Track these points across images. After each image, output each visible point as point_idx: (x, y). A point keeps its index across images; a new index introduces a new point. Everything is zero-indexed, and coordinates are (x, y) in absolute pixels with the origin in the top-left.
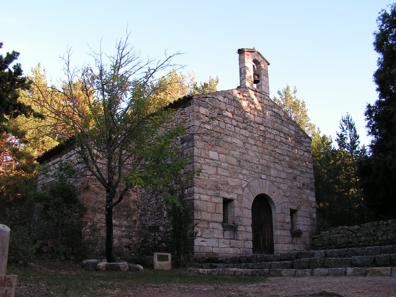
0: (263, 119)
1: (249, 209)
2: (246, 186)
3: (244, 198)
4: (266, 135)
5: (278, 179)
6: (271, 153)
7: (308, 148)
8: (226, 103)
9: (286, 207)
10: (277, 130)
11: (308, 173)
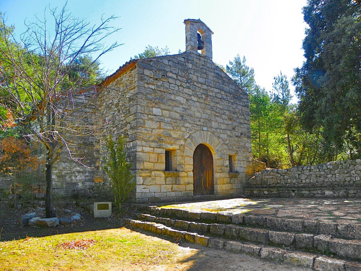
0: (206, 79)
1: (191, 157)
2: (188, 137)
3: (186, 148)
4: (209, 93)
5: (218, 130)
6: (213, 108)
7: (246, 103)
8: (170, 66)
9: (226, 153)
10: (218, 89)
11: (245, 124)
